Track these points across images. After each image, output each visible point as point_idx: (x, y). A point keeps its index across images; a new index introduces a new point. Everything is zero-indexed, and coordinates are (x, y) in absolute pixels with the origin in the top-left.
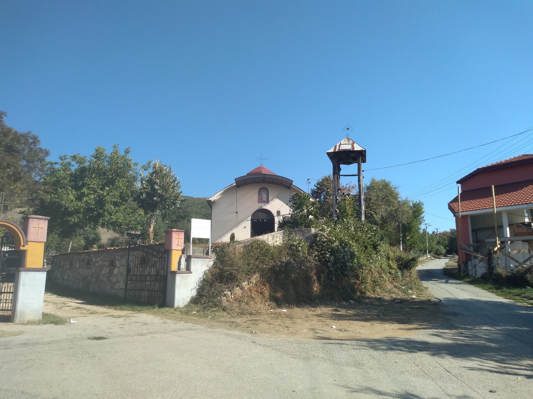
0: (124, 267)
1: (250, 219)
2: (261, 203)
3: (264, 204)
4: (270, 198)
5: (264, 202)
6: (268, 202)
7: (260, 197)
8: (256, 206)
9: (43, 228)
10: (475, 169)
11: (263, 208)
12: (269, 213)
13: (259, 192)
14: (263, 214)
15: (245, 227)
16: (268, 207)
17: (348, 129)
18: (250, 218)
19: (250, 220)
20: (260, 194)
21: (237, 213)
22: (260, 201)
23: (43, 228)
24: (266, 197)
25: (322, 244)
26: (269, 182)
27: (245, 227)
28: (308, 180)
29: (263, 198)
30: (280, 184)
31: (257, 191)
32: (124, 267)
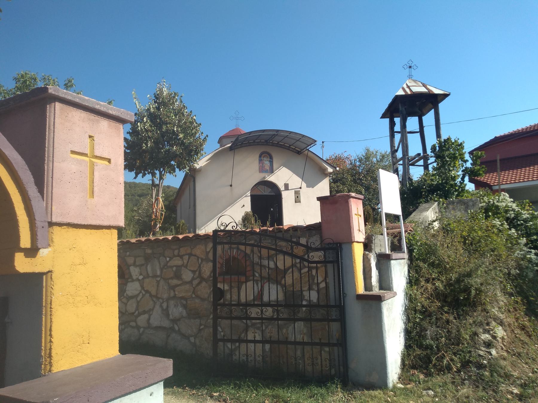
0: (158, 282)
1: (249, 195)
2: (263, 172)
3: (268, 174)
4: (275, 166)
5: (266, 171)
6: (272, 171)
7: (261, 165)
8: (257, 177)
9: (109, 161)
10: (493, 137)
11: (266, 179)
12: (273, 186)
13: (260, 156)
14: (265, 187)
15: (244, 206)
16: (272, 178)
17: (410, 67)
18: (249, 194)
19: (249, 196)
20: (260, 160)
21: (231, 186)
22: (262, 170)
23: (109, 161)
24: (269, 165)
25: (522, 224)
26: (273, 145)
27: (244, 206)
28: (323, 142)
29: (265, 166)
30: (287, 148)
31: (258, 156)
32: (158, 282)
